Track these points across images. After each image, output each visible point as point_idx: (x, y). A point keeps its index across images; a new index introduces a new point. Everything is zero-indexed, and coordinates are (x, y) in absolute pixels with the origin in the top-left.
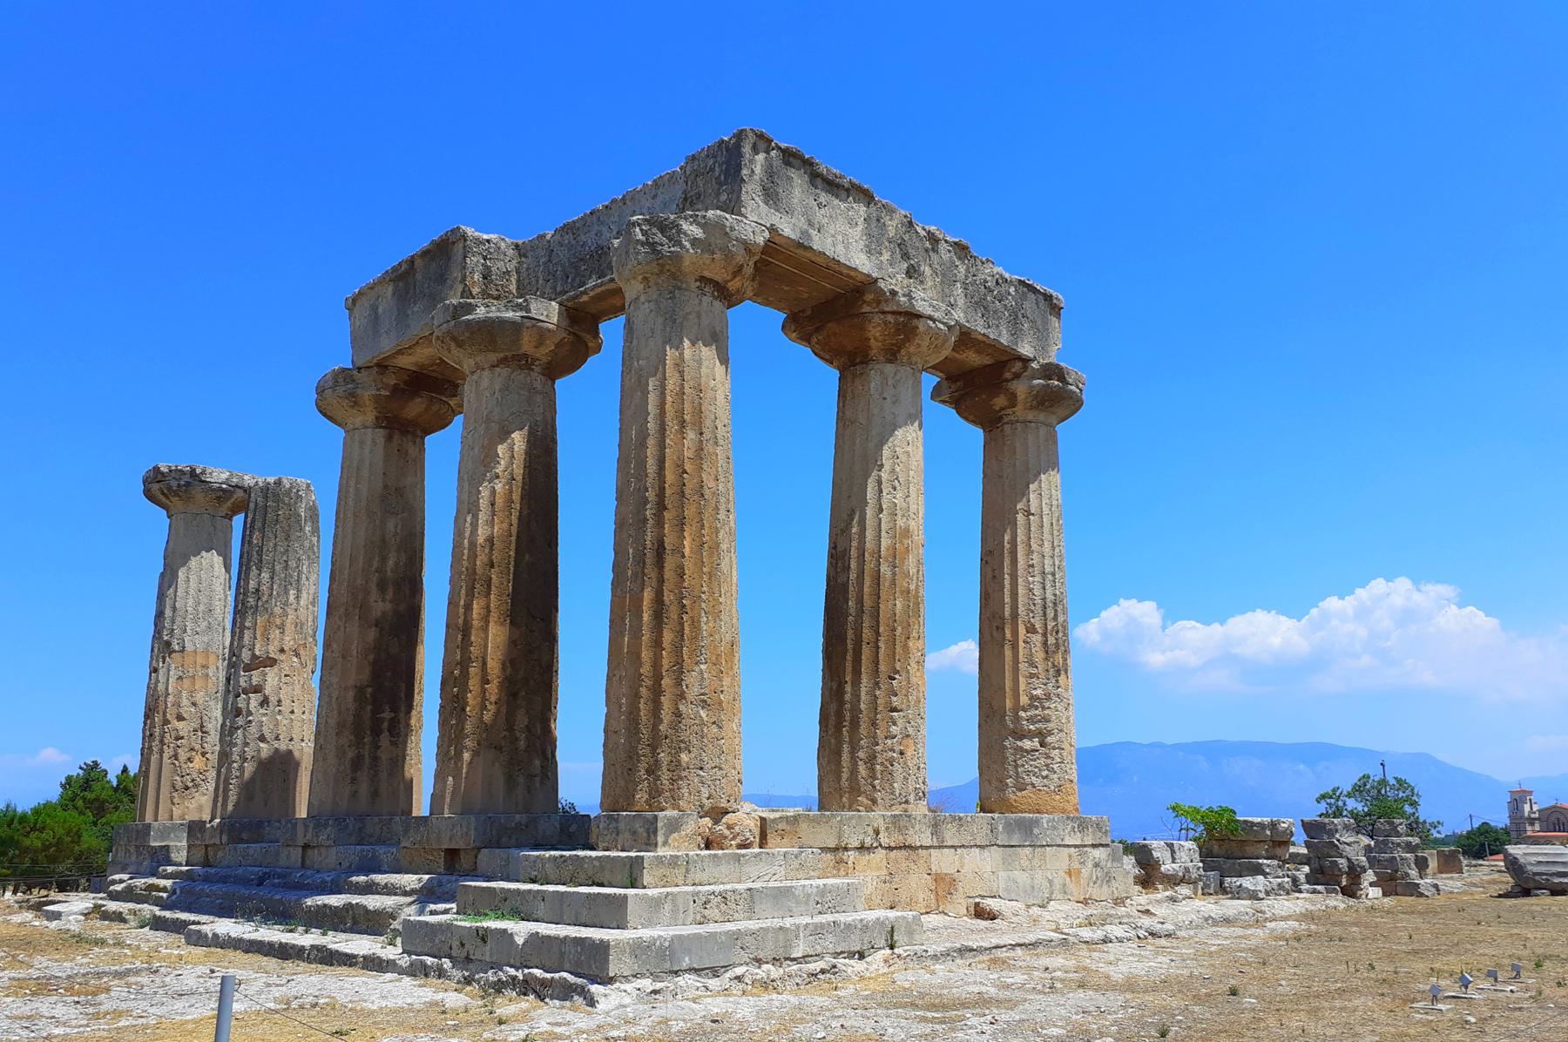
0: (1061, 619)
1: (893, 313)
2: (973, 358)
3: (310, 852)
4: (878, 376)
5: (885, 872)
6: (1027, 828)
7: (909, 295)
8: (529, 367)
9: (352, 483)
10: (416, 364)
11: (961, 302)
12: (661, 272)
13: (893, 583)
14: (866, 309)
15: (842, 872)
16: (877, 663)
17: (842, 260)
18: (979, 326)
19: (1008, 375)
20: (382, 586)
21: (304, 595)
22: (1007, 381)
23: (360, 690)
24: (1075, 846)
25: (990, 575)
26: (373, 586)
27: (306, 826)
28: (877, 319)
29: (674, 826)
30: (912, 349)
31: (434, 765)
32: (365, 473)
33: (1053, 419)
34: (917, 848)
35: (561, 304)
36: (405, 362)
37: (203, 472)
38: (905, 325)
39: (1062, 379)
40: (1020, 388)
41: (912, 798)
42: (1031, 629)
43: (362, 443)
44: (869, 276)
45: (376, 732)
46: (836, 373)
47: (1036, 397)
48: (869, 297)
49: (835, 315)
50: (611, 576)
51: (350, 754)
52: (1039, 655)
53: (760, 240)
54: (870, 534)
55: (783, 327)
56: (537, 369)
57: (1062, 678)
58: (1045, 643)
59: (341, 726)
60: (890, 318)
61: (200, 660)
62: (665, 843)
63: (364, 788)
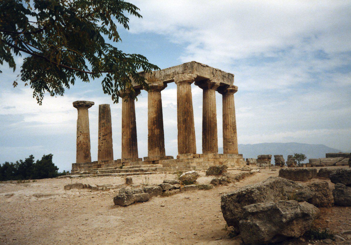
1: (212, 83)
3: (124, 164)
13: (213, 121)
14: (208, 82)
16: (211, 133)
18: (223, 82)
20: (132, 123)
23: (130, 139)
26: (130, 123)
27: (123, 160)
33: (233, 93)
39: (235, 88)
42: (231, 126)
45: (133, 145)
49: (202, 82)
52: (232, 130)
53: (196, 77)
54: (209, 114)
58: (233, 128)
59: (127, 145)
63: (132, 154)
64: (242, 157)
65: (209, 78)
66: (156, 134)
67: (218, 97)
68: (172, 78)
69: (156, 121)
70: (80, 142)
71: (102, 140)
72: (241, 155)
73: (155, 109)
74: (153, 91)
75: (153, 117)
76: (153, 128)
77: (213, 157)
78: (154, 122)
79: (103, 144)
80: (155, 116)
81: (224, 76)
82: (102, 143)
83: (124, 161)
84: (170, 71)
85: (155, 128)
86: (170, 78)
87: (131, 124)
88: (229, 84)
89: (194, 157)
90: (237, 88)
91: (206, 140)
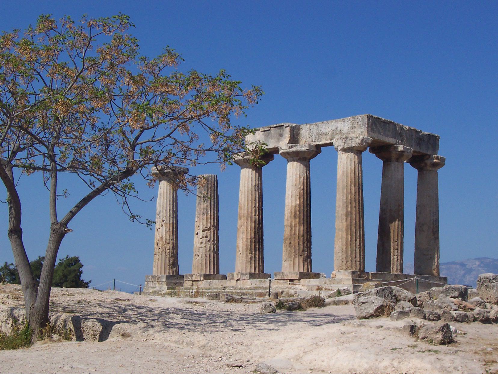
2: (416, 154)
9: (246, 182)
18: (418, 149)
23: (251, 239)
32: (250, 179)
48: (392, 147)
51: (249, 256)
52: (432, 234)
58: (433, 231)
59: (247, 249)
67: (410, 174)
68: (331, 140)
69: (299, 211)
70: (162, 238)
73: (298, 191)
75: (294, 204)
76: (293, 224)
79: (203, 245)
80: (298, 203)
81: (421, 139)
82: (201, 243)
83: (239, 277)
86: (327, 140)
87: (254, 214)
88: (429, 153)
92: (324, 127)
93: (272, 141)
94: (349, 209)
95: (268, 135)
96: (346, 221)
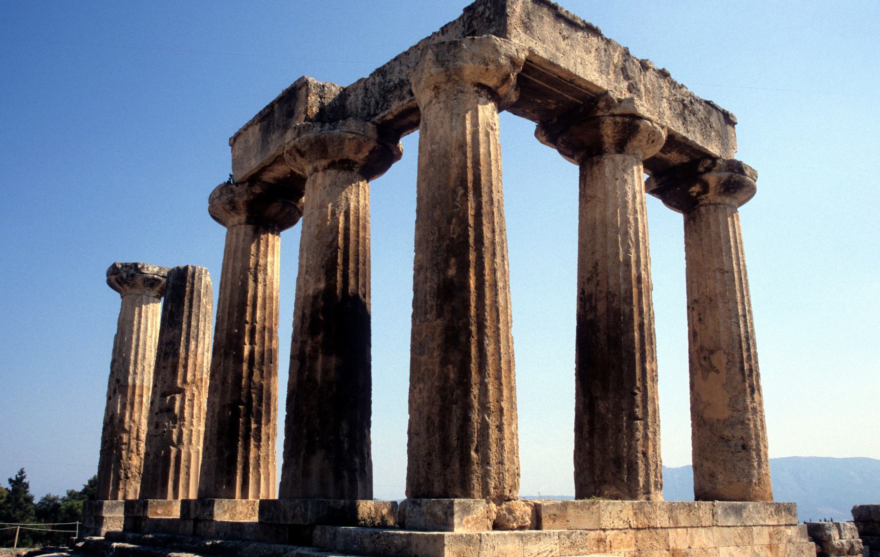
0: (752, 350)
1: (622, 115)
2: (674, 157)
4: (610, 163)
5: (633, 549)
6: (738, 511)
7: (631, 100)
8: (350, 169)
10: (275, 179)
11: (668, 113)
12: (448, 81)
14: (600, 113)
15: (602, 549)
17: (582, 76)
19: (701, 169)
21: (200, 346)
22: (702, 173)
24: (774, 526)
25: (696, 318)
28: (609, 120)
29: (466, 510)
30: (635, 143)
31: (282, 462)
33: (734, 203)
34: (657, 528)
35: (374, 123)
36: (268, 177)
37: (143, 267)
38: (630, 124)
40: (712, 179)
41: (652, 489)
43: (237, 234)
44: (600, 88)
46: (578, 167)
47: (724, 184)
48: (602, 104)
49: (575, 120)
50: (411, 310)
53: (523, 56)
55: (536, 134)
56: (357, 170)
57: (756, 395)
60: (618, 119)
61: (137, 392)
62: (460, 524)
64: (794, 521)
65: (606, 88)
66: (319, 376)
71: (157, 414)
72: (789, 509)
74: (325, 169)
75: (311, 292)
76: (308, 349)
77: (634, 524)
78: (314, 315)
81: (685, 106)
83: (198, 513)
84: (404, 68)
85: (315, 350)
88: (714, 149)
89: (496, 526)
90: (754, 175)
91: (591, 422)
92: (397, 69)
93: (274, 137)
94: (452, 272)
95: (269, 127)
96: (439, 315)
